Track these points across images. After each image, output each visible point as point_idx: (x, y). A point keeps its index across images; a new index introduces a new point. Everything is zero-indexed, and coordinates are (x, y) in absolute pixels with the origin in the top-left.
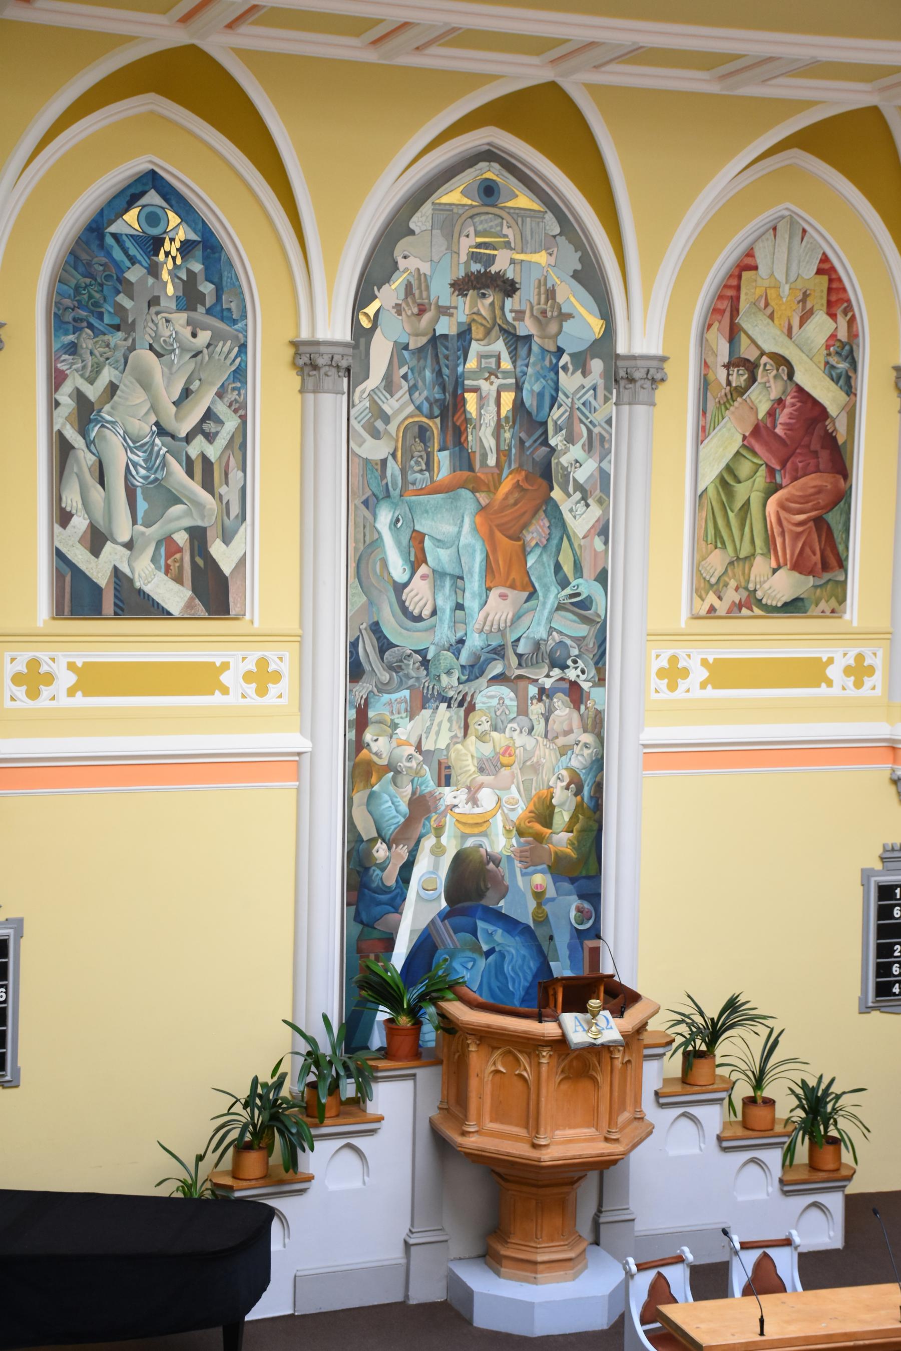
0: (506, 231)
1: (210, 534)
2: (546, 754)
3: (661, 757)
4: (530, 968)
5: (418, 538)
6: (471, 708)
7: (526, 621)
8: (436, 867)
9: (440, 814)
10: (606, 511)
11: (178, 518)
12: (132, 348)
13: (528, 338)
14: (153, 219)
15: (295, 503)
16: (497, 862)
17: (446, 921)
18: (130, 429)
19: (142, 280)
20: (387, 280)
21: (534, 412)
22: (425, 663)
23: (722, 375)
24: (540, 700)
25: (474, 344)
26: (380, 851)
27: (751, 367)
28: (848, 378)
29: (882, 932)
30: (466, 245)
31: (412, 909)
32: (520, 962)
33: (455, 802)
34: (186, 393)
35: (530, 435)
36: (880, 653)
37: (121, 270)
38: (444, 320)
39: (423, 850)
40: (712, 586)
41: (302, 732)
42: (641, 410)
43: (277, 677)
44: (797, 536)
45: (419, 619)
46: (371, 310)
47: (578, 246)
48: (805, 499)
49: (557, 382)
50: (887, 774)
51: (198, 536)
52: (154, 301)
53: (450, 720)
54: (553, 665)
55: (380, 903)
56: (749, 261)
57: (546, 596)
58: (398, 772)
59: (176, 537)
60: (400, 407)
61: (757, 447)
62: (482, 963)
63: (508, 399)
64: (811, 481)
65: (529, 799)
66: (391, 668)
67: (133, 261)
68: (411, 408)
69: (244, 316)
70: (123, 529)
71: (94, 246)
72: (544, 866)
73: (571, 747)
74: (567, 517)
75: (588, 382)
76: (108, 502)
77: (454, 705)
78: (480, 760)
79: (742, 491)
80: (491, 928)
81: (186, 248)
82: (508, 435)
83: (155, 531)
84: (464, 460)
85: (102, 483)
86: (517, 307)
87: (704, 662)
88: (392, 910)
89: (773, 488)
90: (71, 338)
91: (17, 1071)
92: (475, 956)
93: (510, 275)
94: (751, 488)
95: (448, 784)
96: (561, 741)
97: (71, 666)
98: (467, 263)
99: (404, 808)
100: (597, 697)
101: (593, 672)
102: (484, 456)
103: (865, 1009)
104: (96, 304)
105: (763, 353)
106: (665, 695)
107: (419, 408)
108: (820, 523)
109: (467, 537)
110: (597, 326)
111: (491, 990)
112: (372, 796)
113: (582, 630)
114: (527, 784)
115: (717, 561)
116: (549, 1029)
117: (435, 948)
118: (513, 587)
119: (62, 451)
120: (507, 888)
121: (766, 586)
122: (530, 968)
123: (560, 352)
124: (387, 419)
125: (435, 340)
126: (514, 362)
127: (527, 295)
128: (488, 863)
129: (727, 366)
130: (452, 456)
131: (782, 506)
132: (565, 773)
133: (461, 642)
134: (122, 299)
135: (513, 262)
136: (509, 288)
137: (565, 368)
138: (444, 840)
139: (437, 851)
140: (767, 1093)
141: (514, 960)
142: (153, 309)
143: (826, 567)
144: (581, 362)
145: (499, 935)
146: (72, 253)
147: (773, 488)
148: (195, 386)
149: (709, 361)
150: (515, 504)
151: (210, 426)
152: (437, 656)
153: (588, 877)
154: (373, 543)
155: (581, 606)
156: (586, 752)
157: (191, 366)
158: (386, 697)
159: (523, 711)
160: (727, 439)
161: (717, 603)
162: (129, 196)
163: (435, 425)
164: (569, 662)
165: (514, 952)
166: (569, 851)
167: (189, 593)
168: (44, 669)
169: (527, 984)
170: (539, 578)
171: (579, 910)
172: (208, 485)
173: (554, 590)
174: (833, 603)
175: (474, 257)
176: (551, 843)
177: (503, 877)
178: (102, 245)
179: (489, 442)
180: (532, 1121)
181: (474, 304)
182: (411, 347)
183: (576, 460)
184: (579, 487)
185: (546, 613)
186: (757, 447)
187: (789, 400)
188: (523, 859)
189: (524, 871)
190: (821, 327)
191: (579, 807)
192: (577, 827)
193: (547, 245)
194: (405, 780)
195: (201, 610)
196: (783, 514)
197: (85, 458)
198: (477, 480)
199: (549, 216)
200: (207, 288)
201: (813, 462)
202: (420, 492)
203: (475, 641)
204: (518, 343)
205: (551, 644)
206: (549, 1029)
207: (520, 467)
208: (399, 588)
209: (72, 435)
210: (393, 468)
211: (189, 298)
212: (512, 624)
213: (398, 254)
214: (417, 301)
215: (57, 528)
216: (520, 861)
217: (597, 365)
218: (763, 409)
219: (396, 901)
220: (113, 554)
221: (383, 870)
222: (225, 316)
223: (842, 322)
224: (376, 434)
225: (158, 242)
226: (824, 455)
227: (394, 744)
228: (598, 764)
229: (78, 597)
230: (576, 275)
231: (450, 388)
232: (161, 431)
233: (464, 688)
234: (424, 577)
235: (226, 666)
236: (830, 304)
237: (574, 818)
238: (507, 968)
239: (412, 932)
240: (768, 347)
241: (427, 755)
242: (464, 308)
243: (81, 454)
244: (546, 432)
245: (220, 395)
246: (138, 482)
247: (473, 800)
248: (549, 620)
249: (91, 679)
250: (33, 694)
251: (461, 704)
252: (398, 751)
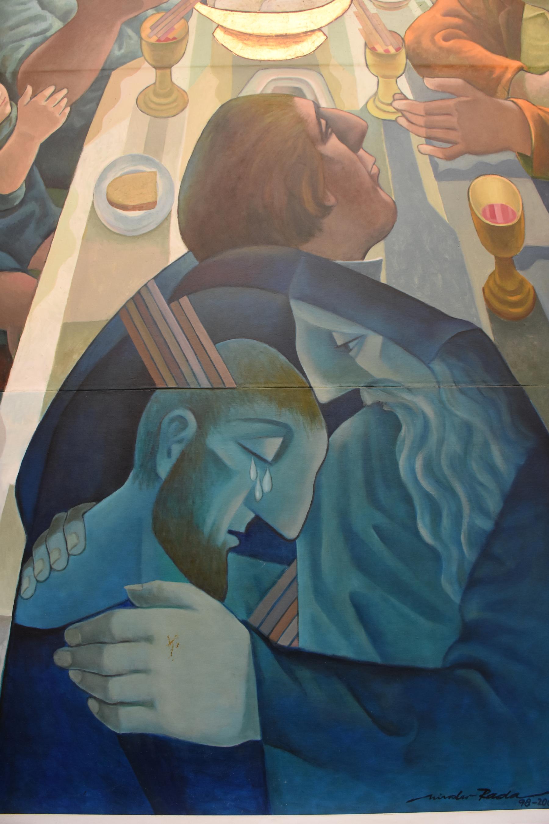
4: (492, 469)
9: (168, 10)
16: (354, 137)
17: (185, 301)
31: (72, 261)
32: (453, 443)
39: (116, 99)
62: (315, 444)
72: (510, 156)
80: (343, 330)
88: (12, 263)
92: (287, 417)
111: (349, 534)
117: (142, 389)
120: (393, 211)
122: (492, 469)
128: (324, 138)
138: (181, 75)
139: (163, 102)
141: (434, 438)
145: (373, 354)
165: (429, 410)
169: (486, 524)
176: (525, 97)
177: (375, 179)
188: (439, 133)
189: (443, 165)
216: (429, 139)
238: (410, 465)
239: (68, 330)
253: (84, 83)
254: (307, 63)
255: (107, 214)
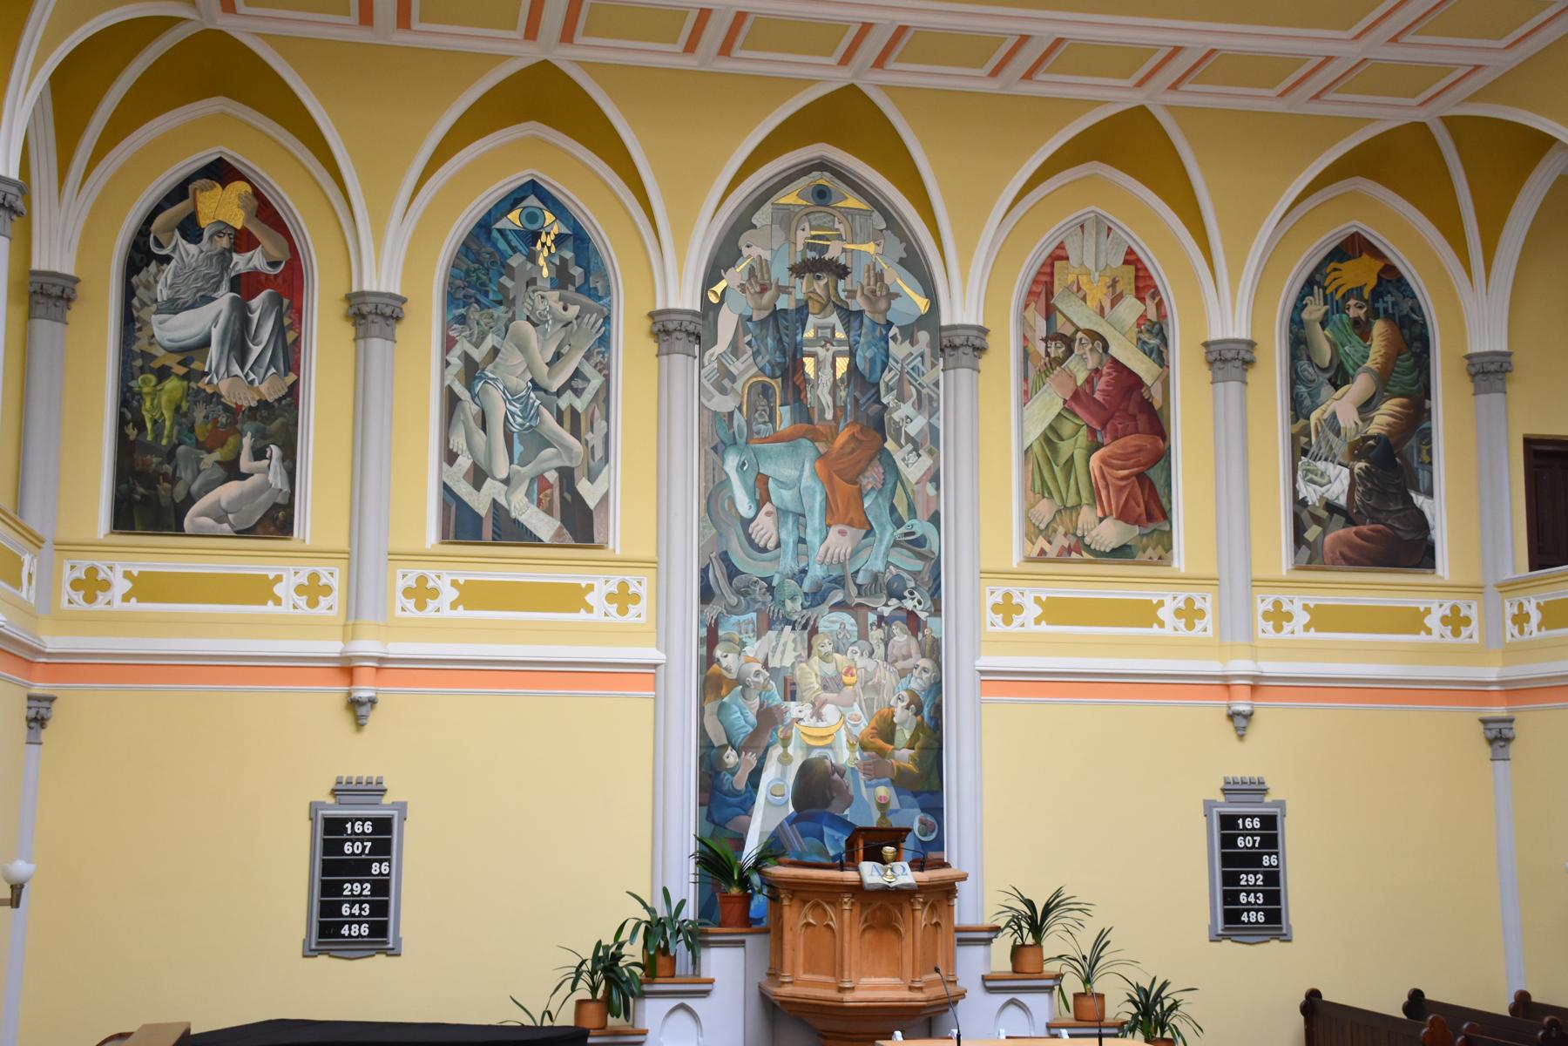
0: (837, 226)
1: (576, 473)
2: (886, 676)
3: (995, 680)
5: (762, 480)
6: (814, 631)
7: (864, 555)
8: (783, 775)
10: (937, 461)
11: (550, 459)
12: (512, 319)
13: (860, 313)
14: (532, 217)
15: (651, 447)
18: (509, 385)
19: (522, 265)
20: (733, 265)
21: (867, 373)
22: (771, 589)
23: (1041, 347)
24: (879, 626)
25: (811, 317)
26: (731, 757)
27: (1068, 342)
28: (1160, 353)
29: (1227, 860)
30: (802, 237)
33: (801, 715)
34: (558, 356)
35: (863, 394)
36: (1209, 598)
37: (504, 257)
38: (783, 297)
40: (1041, 531)
41: (657, 647)
42: (964, 373)
43: (636, 598)
44: (1120, 489)
45: (764, 550)
46: (719, 288)
47: (903, 237)
48: (1126, 456)
49: (887, 350)
50: (1224, 711)
51: (567, 475)
52: (532, 282)
53: (794, 641)
54: (890, 596)
55: (730, 805)
56: (1060, 252)
57: (882, 534)
58: (746, 686)
59: (547, 475)
60: (745, 369)
61: (1077, 410)
63: (842, 364)
64: (1131, 441)
65: (870, 716)
66: (738, 592)
67: (515, 250)
68: (755, 369)
69: (608, 292)
70: (502, 468)
71: (483, 240)
73: (910, 671)
74: (901, 465)
75: (916, 350)
76: (489, 445)
77: (798, 628)
78: (823, 679)
79: (1065, 448)
81: (560, 240)
82: (843, 394)
83: (529, 470)
84: (804, 413)
85: (484, 429)
86: (849, 287)
87: (1038, 600)
89: (1095, 447)
90: (462, 311)
91: (398, 940)
93: (842, 261)
94: (1074, 445)
95: (793, 699)
96: (900, 664)
97: (454, 583)
98: (803, 252)
99: (752, 718)
100: (934, 626)
101: (929, 603)
102: (822, 411)
103: (1216, 938)
104: (483, 284)
105: (1078, 330)
106: (1001, 627)
107: (762, 369)
108: (1142, 478)
109: (807, 480)
110: (922, 304)
112: (722, 706)
113: (918, 565)
114: (869, 703)
115: (1045, 510)
116: (850, 876)
118: (851, 524)
119: (451, 402)
121: (1094, 533)
123: (889, 325)
124: (733, 379)
125: (776, 314)
126: (847, 333)
127: (859, 277)
129: (1045, 340)
130: (793, 412)
131: (1104, 461)
132: (904, 694)
133: (804, 571)
134: (505, 280)
135: (844, 250)
136: (842, 272)
137: (894, 338)
138: (790, 750)
139: (785, 760)
140: (1098, 987)
142: (531, 288)
143: (1150, 518)
144: (909, 333)
146: (464, 244)
147: (1095, 447)
148: (565, 350)
149: (1028, 335)
150: (852, 452)
151: (578, 383)
152: (781, 583)
153: (931, 793)
154: (722, 482)
155: (916, 544)
156: (925, 676)
157: (562, 334)
158: (734, 618)
159: (863, 635)
160: (1048, 404)
161: (1047, 547)
162: (513, 200)
163: (777, 385)
164: (906, 594)
166: (911, 766)
167: (557, 523)
168: (430, 584)
170: (876, 518)
171: (922, 822)
172: (576, 432)
173: (890, 528)
174: (1160, 550)
175: (809, 246)
178: (489, 238)
179: (827, 399)
180: (837, 968)
181: (810, 284)
182: (755, 318)
183: (906, 416)
184: (909, 439)
185: (883, 548)
186: (1077, 410)
187: (1105, 370)
190: (1130, 309)
191: (919, 727)
192: (918, 745)
193: (875, 236)
194: (753, 693)
195: (569, 540)
196: (1106, 470)
197: (470, 408)
198: (815, 430)
199: (876, 214)
200: (577, 271)
201: (1132, 424)
202: (765, 440)
203: (817, 571)
204: (850, 317)
205: (888, 576)
206: (850, 876)
207: (856, 421)
208: (746, 523)
209: (459, 389)
210: (739, 420)
211: (561, 279)
212: (852, 556)
213: (742, 244)
214: (759, 280)
215: (445, 466)
217: (923, 337)
218: (1080, 380)
219: (746, 804)
220: (492, 488)
221: (733, 774)
222: (592, 293)
223: (1151, 305)
224: (723, 391)
225: (535, 236)
226: (1142, 420)
227: (743, 660)
228: (936, 687)
229: (462, 525)
230: (901, 262)
231: (790, 353)
232: (536, 387)
233: (807, 613)
234: (768, 514)
235: (590, 588)
236: (1137, 289)
237: (915, 737)
239: (761, 834)
240: (1082, 325)
241: (774, 672)
242: (801, 288)
243: (467, 405)
244: (878, 391)
245: (587, 357)
246: (515, 428)
247: (818, 715)
248: (887, 555)
249: (472, 595)
250: (421, 606)
251: (804, 627)
252: (746, 667)
253: (761, 752)
254: (829, 747)
255: (771, 798)
